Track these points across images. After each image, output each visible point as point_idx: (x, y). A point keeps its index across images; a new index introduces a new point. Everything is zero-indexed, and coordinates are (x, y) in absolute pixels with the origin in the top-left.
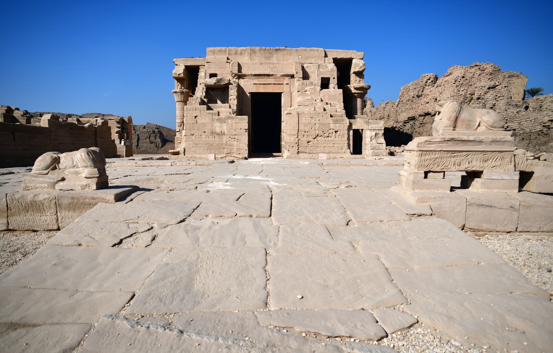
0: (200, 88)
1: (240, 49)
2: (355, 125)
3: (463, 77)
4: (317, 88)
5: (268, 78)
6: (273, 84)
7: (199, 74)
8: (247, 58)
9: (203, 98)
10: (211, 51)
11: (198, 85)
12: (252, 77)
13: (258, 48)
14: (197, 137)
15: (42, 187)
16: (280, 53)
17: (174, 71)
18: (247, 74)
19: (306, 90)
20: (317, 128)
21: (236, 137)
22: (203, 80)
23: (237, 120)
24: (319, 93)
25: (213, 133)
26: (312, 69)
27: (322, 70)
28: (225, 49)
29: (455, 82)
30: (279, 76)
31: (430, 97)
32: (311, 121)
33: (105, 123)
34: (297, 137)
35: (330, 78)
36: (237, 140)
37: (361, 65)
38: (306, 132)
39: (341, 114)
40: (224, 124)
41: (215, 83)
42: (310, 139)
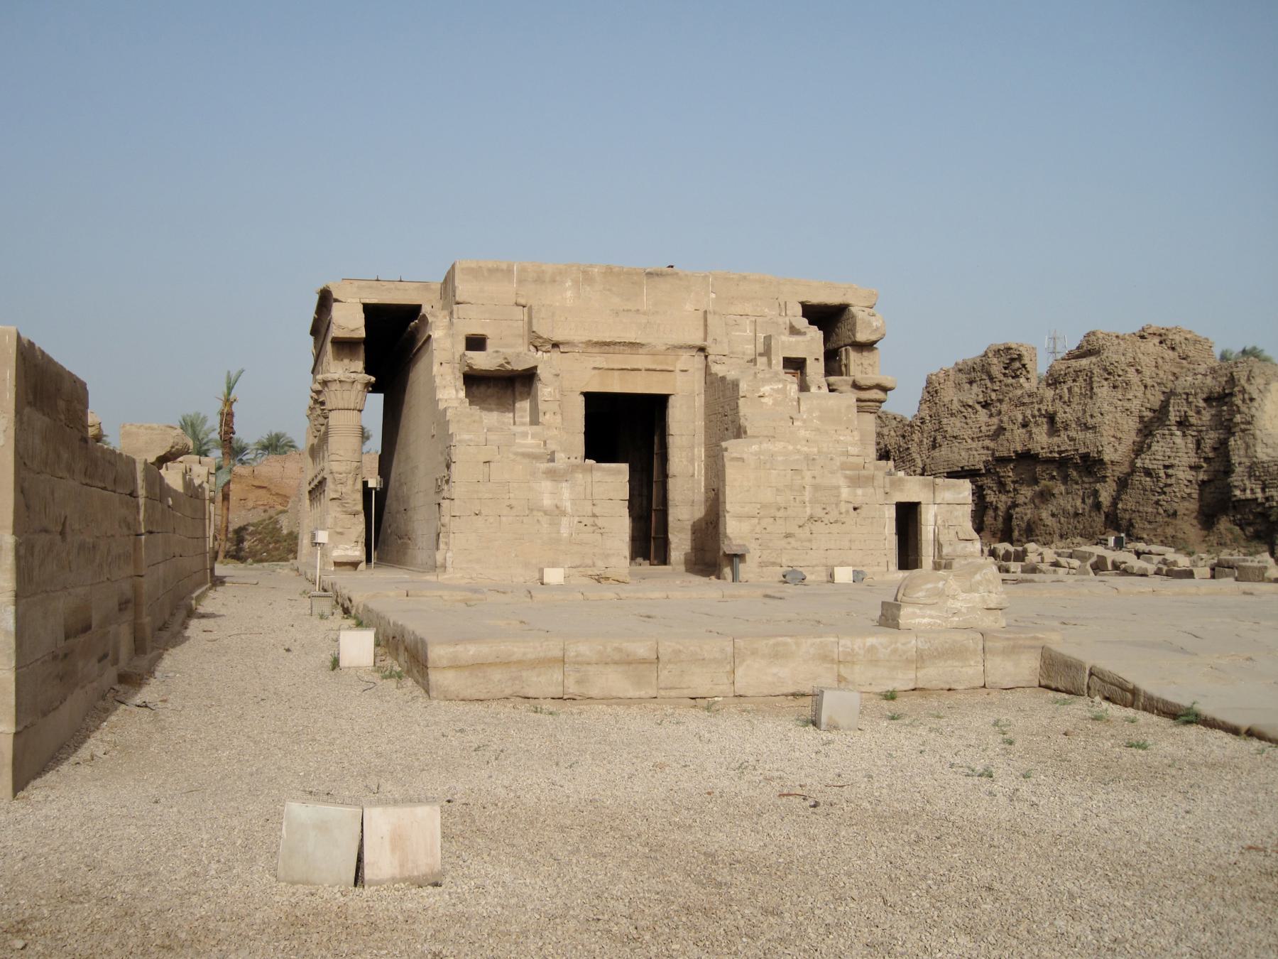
2: (902, 490)
4: (791, 388)
5: (633, 352)
6: (648, 370)
8: (569, 294)
12: (590, 350)
14: (491, 520)
19: (761, 394)
20: (807, 499)
23: (599, 474)
24: (795, 403)
25: (531, 510)
29: (1107, 376)
30: (664, 348)
32: (792, 480)
34: (759, 523)
39: (860, 460)
40: (564, 484)
41: (501, 365)
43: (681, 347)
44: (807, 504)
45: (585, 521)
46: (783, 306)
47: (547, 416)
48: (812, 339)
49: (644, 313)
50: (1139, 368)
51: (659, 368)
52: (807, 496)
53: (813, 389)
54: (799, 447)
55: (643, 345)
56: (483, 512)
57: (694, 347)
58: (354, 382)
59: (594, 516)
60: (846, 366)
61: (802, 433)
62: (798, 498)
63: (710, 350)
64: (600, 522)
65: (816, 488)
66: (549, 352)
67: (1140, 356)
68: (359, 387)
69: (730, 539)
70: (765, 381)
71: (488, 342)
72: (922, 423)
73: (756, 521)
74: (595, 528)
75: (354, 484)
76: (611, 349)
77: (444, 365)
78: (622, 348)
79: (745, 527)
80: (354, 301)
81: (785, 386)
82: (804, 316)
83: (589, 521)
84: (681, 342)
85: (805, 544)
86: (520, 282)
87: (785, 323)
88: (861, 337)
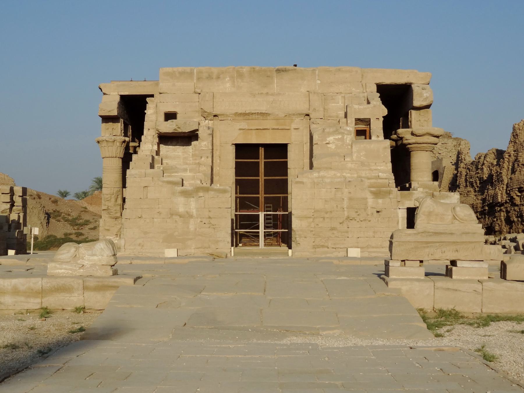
1: (215, 71)
4: (347, 138)
6: (273, 129)
7: (145, 111)
8: (228, 85)
10: (168, 74)
15: (65, 273)
19: (328, 142)
23: (212, 193)
24: (350, 147)
25: (172, 215)
26: (340, 103)
27: (356, 107)
28: (191, 70)
30: (284, 116)
34: (313, 222)
36: (213, 227)
38: (327, 213)
40: (192, 199)
41: (175, 130)
43: (294, 115)
44: (346, 209)
46: (364, 86)
47: (203, 159)
48: (375, 106)
49: (272, 95)
51: (280, 127)
52: (345, 204)
53: (373, 138)
54: (344, 174)
55: (270, 114)
56: (143, 216)
59: (210, 218)
60: (410, 122)
63: (311, 116)
64: (213, 221)
65: (350, 199)
68: (118, 144)
69: (295, 231)
70: (330, 134)
71: (178, 116)
73: (311, 220)
74: (209, 225)
75: (116, 201)
76: (250, 117)
77: (150, 130)
78: (257, 116)
79: (305, 223)
80: (115, 94)
82: (377, 92)
86: (199, 79)
87: (364, 97)
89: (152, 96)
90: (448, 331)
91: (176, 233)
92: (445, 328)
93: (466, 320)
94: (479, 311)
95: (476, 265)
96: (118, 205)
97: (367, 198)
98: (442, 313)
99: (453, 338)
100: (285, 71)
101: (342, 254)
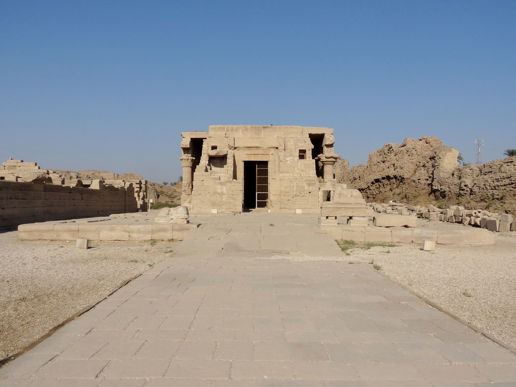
0: (204, 158)
2: (324, 187)
3: (413, 148)
4: (295, 159)
7: (203, 146)
8: (241, 134)
9: (207, 166)
11: (202, 155)
13: (249, 126)
16: (267, 130)
17: (182, 143)
18: (241, 146)
19: (287, 160)
21: (233, 196)
22: (206, 151)
23: (234, 183)
24: (297, 163)
25: (215, 193)
26: (292, 142)
27: (300, 144)
29: (407, 152)
31: (390, 163)
32: (290, 184)
33: (131, 185)
34: (280, 197)
35: (306, 150)
37: (331, 139)
38: (286, 193)
39: (313, 179)
40: (224, 186)
41: (216, 154)
42: (290, 198)
43: (271, 148)
44: (295, 191)
45: (230, 196)
47: (229, 168)
49: (261, 138)
50: (416, 149)
53: (308, 159)
54: (294, 175)
57: (275, 148)
58: (188, 159)
59: (232, 195)
61: (297, 171)
62: (292, 190)
65: (297, 186)
66: (234, 150)
67: (417, 146)
68: (190, 161)
70: (287, 157)
71: (218, 148)
72: (367, 168)
75: (189, 187)
81: (294, 158)
83: (231, 196)
84: (271, 146)
85: (294, 202)
86: (227, 131)
88: (327, 143)
89: (206, 138)
90: (351, 252)
91: (217, 202)
92: (350, 250)
93: (358, 245)
94: (364, 241)
95: (362, 219)
96: (190, 188)
97: (304, 186)
98: (346, 242)
99: (355, 256)
100: (267, 127)
101: (293, 211)
